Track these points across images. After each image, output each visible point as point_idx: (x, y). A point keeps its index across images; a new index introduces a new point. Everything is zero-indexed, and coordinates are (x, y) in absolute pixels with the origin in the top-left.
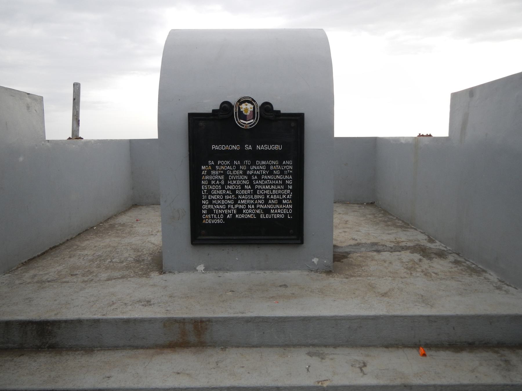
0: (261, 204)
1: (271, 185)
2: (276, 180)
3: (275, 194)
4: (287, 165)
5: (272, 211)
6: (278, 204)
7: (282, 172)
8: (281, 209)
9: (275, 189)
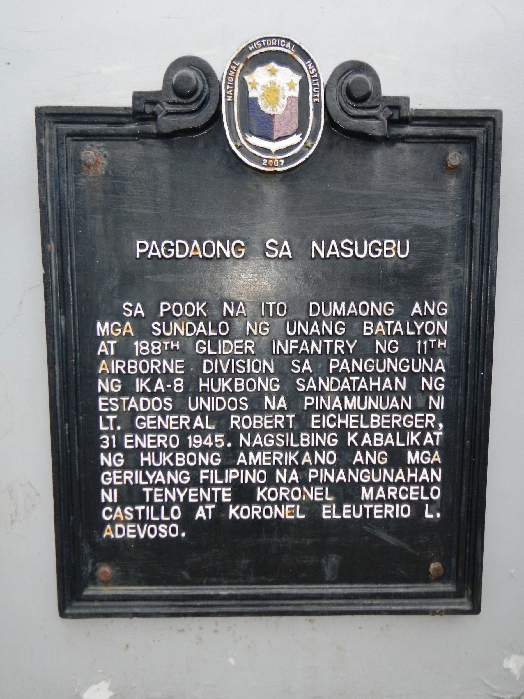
0: (326, 465)
1: (363, 393)
2: (382, 376)
3: (380, 429)
4: (429, 316)
5: (366, 494)
6: (388, 466)
7: (408, 347)
8: (399, 483)
9: (380, 412)
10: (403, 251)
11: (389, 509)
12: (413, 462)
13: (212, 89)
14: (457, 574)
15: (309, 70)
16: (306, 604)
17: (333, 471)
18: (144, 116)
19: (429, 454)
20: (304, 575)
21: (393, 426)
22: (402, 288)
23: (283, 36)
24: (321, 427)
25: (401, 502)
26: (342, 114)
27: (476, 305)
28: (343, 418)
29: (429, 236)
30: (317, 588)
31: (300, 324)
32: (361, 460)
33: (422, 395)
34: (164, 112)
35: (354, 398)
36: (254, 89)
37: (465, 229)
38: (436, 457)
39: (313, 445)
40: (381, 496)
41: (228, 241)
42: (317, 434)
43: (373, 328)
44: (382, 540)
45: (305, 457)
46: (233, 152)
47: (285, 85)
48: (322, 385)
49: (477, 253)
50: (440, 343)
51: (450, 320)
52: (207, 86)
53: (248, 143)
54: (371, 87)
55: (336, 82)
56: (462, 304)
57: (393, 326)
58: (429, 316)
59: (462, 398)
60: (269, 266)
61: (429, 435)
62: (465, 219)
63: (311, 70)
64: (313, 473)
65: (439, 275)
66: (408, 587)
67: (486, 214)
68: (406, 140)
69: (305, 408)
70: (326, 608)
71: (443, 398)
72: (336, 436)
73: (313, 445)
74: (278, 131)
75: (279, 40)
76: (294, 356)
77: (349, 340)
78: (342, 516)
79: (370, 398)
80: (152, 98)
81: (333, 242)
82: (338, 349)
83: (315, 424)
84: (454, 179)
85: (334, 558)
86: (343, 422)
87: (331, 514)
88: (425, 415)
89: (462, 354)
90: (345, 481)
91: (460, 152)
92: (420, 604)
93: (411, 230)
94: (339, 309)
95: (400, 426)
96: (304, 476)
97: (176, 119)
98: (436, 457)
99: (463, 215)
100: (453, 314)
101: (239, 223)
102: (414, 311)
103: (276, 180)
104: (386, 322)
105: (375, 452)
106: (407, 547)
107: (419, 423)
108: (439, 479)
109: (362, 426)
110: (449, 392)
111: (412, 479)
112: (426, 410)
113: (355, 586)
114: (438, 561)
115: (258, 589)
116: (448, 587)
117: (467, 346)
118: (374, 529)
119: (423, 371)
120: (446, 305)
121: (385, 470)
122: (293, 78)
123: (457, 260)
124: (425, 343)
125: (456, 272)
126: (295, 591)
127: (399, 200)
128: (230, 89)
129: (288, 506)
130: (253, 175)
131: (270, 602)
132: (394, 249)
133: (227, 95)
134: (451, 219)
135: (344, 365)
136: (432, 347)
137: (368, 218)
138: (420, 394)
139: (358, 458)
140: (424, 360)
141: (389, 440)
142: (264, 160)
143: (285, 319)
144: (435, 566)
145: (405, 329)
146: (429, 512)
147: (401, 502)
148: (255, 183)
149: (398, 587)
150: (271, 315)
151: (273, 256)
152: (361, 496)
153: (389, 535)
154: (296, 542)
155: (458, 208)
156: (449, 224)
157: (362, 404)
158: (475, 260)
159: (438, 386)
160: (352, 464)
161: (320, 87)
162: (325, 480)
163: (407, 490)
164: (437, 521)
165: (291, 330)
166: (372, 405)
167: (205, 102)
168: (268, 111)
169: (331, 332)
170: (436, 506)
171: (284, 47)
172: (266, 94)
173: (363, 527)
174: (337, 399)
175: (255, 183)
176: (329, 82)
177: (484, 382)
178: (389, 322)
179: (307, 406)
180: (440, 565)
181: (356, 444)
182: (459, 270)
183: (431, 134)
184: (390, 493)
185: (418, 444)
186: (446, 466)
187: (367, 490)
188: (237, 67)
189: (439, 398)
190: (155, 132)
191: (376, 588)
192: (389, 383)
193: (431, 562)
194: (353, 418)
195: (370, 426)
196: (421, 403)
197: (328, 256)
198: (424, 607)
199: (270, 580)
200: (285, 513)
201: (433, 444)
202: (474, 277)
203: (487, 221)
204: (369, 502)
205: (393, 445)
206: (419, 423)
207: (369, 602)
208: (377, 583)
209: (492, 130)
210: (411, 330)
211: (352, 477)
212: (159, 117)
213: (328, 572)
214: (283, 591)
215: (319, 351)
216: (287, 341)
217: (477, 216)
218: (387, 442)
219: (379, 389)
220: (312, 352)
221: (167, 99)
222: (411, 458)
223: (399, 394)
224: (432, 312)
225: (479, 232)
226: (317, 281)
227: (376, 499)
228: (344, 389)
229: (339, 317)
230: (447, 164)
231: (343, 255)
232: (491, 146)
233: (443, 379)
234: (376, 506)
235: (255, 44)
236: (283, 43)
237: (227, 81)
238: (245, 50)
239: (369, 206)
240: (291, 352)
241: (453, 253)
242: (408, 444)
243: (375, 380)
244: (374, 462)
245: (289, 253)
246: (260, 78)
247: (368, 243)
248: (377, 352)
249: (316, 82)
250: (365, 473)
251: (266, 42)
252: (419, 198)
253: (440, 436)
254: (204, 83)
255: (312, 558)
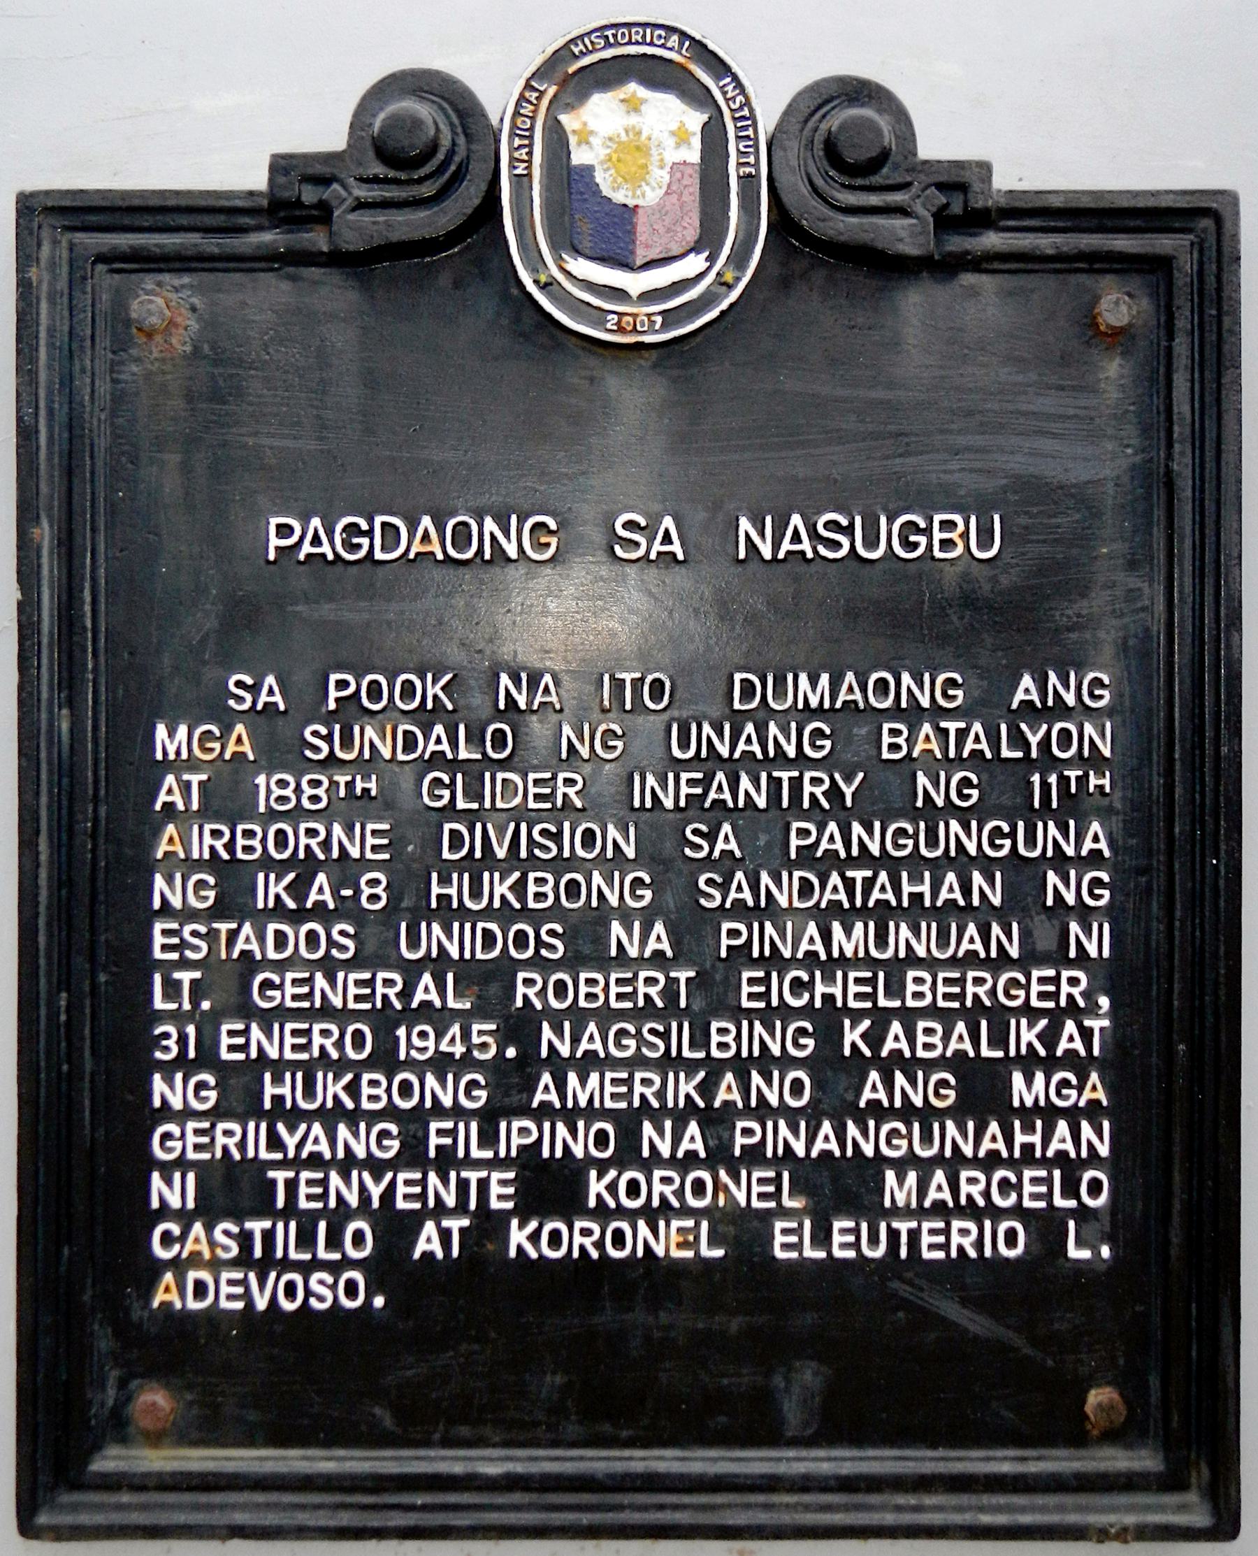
0: (784, 1110)
1: (883, 915)
2: (938, 867)
3: (932, 1011)
4: (1061, 710)
5: (898, 1189)
6: (958, 1113)
7: (1007, 790)
8: (992, 1161)
9: (931, 964)
10: (985, 543)
11: (964, 1232)
12: (1029, 1102)
13: (474, 147)
14: (1167, 1420)
15: (727, 100)
16: (730, 1506)
17: (803, 1124)
18: (297, 213)
19: (1074, 1081)
20: (722, 1419)
21: (969, 1003)
22: (985, 636)
23: (660, 21)
24: (769, 1003)
25: (997, 1214)
26: (815, 203)
27: (1188, 681)
28: (829, 979)
29: (1055, 503)
30: (761, 1459)
31: (707, 729)
32: (881, 1095)
33: (1049, 919)
34: (350, 202)
35: (859, 926)
36: (584, 147)
37: (1150, 487)
38: (1094, 1088)
39: (745, 1054)
40: (940, 1196)
41: (514, 518)
42: (757, 1024)
43: (907, 740)
44: (944, 1320)
45: (724, 1086)
46: (529, 296)
47: (666, 134)
48: (768, 891)
49: (1185, 547)
50: (1093, 781)
51: (1119, 719)
52: (461, 140)
53: (568, 274)
54: (888, 138)
55: (798, 126)
56: (1151, 677)
57: (962, 734)
58: (1061, 710)
59: (1162, 927)
60: (624, 581)
61: (1070, 1027)
62: (1151, 460)
63: (733, 99)
64: (747, 1132)
65: (1085, 603)
66: (1023, 1459)
67: (1207, 448)
68: (985, 266)
69: (723, 954)
70: (786, 1518)
71: (1106, 927)
72: (811, 1029)
73: (745, 1054)
74: (647, 246)
75: (648, 31)
76: (691, 813)
77: (840, 773)
78: (830, 1253)
79: (903, 926)
80: (319, 169)
81: (796, 520)
82: (812, 795)
83: (751, 996)
84: (1118, 361)
85: (809, 1372)
86: (829, 990)
87: (798, 1247)
88: (1059, 975)
89: (1155, 810)
90: (837, 1153)
91: (1129, 295)
92: (1061, 1509)
93: (1004, 489)
94: (814, 690)
95: (988, 1003)
96: (720, 1138)
97: (381, 219)
98: (1094, 1088)
99: (1143, 451)
100: (1127, 703)
101: (543, 473)
102: (1020, 696)
103: (641, 366)
104: (943, 724)
105: (920, 1074)
106: (1018, 1340)
107: (1042, 996)
108: (1104, 1150)
109: (883, 1002)
110: (1124, 910)
111: (1028, 1148)
112: (1060, 958)
113: (871, 1453)
114: (1109, 1383)
115: (591, 1459)
116: (1140, 1459)
117: (1169, 788)
118: (922, 1290)
119: (1050, 853)
120: (1107, 681)
121: (950, 1125)
122: (685, 119)
123: (1132, 565)
124: (1053, 779)
125: (1132, 595)
126: (696, 1468)
127: (970, 414)
128: (520, 147)
129: (675, 1224)
130: (580, 352)
131: (626, 1499)
132: (961, 536)
133: (512, 159)
134: (1112, 460)
135: (831, 839)
136: (1073, 790)
137: (887, 457)
138: (1043, 917)
139: (872, 1090)
140: (1051, 824)
141: (961, 1041)
142: (610, 317)
143: (666, 716)
144: (1100, 1398)
145: (996, 747)
146: (1080, 1243)
147: (997, 1214)
148: (588, 373)
149: (995, 1459)
150: (628, 706)
151: (634, 556)
152: (882, 1197)
153: (964, 1307)
154: (701, 1326)
155: (1131, 432)
156: (1108, 472)
157: (882, 941)
158: (1181, 565)
159: (1091, 894)
160: (857, 1107)
161: (756, 139)
162: (780, 1151)
163: (1014, 1179)
164: (1103, 1267)
165: (684, 745)
166: (909, 946)
167: (458, 177)
168: (619, 197)
169: (791, 751)
170: (1097, 1225)
171: (663, 46)
172: (615, 157)
173: (890, 1284)
174: (812, 929)
175: (588, 373)
176: (779, 127)
177: (1222, 883)
178: (952, 726)
179: (729, 948)
180: (1116, 1396)
181: (867, 1052)
182: (1139, 589)
183: (1050, 252)
184: (965, 1189)
185: (1042, 1052)
186: (1123, 1111)
187: (901, 1180)
188: (542, 93)
189: (1095, 926)
190: (325, 249)
191: (932, 1459)
192: (956, 887)
193: (1090, 1387)
194: (858, 981)
195: (903, 1002)
196: (1045, 940)
197: (781, 555)
198: (1073, 1518)
199: (624, 1434)
200: (667, 1242)
201: (1083, 1053)
202: (1181, 609)
203: (1210, 465)
204: (907, 1213)
205: (972, 1054)
206: (1042, 996)
207: (913, 1502)
208: (934, 1446)
209: (1212, 240)
210: (1011, 746)
211: (855, 1144)
212: (336, 214)
213: (792, 1412)
214: (661, 1467)
215: (761, 802)
216: (671, 776)
217: (1182, 453)
218: (953, 1045)
219: (927, 903)
220: (741, 804)
221: (361, 171)
222: (1025, 1090)
223: (984, 916)
224: (1070, 699)
225: (1189, 493)
226: (752, 619)
227: (927, 1204)
228: (830, 901)
229: (814, 711)
230: (1097, 325)
231: (822, 551)
232: (1211, 280)
233: (1105, 877)
234: (926, 1226)
235: (587, 40)
236: (660, 37)
237: (514, 126)
238: (562, 54)
239: (891, 428)
240: (682, 803)
241: (1119, 547)
242: (1012, 1053)
243: (916, 878)
244: (918, 1101)
245: (676, 548)
246: (600, 122)
247: (890, 521)
248: (919, 804)
249: (745, 128)
250: (894, 1133)
251: (615, 36)
252: (1024, 407)
253: (1102, 1029)
254: (454, 133)
255: (745, 1371)
